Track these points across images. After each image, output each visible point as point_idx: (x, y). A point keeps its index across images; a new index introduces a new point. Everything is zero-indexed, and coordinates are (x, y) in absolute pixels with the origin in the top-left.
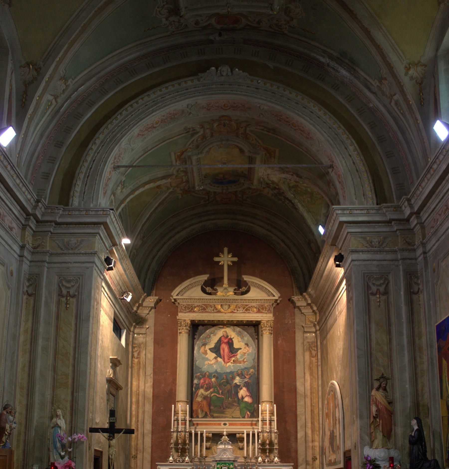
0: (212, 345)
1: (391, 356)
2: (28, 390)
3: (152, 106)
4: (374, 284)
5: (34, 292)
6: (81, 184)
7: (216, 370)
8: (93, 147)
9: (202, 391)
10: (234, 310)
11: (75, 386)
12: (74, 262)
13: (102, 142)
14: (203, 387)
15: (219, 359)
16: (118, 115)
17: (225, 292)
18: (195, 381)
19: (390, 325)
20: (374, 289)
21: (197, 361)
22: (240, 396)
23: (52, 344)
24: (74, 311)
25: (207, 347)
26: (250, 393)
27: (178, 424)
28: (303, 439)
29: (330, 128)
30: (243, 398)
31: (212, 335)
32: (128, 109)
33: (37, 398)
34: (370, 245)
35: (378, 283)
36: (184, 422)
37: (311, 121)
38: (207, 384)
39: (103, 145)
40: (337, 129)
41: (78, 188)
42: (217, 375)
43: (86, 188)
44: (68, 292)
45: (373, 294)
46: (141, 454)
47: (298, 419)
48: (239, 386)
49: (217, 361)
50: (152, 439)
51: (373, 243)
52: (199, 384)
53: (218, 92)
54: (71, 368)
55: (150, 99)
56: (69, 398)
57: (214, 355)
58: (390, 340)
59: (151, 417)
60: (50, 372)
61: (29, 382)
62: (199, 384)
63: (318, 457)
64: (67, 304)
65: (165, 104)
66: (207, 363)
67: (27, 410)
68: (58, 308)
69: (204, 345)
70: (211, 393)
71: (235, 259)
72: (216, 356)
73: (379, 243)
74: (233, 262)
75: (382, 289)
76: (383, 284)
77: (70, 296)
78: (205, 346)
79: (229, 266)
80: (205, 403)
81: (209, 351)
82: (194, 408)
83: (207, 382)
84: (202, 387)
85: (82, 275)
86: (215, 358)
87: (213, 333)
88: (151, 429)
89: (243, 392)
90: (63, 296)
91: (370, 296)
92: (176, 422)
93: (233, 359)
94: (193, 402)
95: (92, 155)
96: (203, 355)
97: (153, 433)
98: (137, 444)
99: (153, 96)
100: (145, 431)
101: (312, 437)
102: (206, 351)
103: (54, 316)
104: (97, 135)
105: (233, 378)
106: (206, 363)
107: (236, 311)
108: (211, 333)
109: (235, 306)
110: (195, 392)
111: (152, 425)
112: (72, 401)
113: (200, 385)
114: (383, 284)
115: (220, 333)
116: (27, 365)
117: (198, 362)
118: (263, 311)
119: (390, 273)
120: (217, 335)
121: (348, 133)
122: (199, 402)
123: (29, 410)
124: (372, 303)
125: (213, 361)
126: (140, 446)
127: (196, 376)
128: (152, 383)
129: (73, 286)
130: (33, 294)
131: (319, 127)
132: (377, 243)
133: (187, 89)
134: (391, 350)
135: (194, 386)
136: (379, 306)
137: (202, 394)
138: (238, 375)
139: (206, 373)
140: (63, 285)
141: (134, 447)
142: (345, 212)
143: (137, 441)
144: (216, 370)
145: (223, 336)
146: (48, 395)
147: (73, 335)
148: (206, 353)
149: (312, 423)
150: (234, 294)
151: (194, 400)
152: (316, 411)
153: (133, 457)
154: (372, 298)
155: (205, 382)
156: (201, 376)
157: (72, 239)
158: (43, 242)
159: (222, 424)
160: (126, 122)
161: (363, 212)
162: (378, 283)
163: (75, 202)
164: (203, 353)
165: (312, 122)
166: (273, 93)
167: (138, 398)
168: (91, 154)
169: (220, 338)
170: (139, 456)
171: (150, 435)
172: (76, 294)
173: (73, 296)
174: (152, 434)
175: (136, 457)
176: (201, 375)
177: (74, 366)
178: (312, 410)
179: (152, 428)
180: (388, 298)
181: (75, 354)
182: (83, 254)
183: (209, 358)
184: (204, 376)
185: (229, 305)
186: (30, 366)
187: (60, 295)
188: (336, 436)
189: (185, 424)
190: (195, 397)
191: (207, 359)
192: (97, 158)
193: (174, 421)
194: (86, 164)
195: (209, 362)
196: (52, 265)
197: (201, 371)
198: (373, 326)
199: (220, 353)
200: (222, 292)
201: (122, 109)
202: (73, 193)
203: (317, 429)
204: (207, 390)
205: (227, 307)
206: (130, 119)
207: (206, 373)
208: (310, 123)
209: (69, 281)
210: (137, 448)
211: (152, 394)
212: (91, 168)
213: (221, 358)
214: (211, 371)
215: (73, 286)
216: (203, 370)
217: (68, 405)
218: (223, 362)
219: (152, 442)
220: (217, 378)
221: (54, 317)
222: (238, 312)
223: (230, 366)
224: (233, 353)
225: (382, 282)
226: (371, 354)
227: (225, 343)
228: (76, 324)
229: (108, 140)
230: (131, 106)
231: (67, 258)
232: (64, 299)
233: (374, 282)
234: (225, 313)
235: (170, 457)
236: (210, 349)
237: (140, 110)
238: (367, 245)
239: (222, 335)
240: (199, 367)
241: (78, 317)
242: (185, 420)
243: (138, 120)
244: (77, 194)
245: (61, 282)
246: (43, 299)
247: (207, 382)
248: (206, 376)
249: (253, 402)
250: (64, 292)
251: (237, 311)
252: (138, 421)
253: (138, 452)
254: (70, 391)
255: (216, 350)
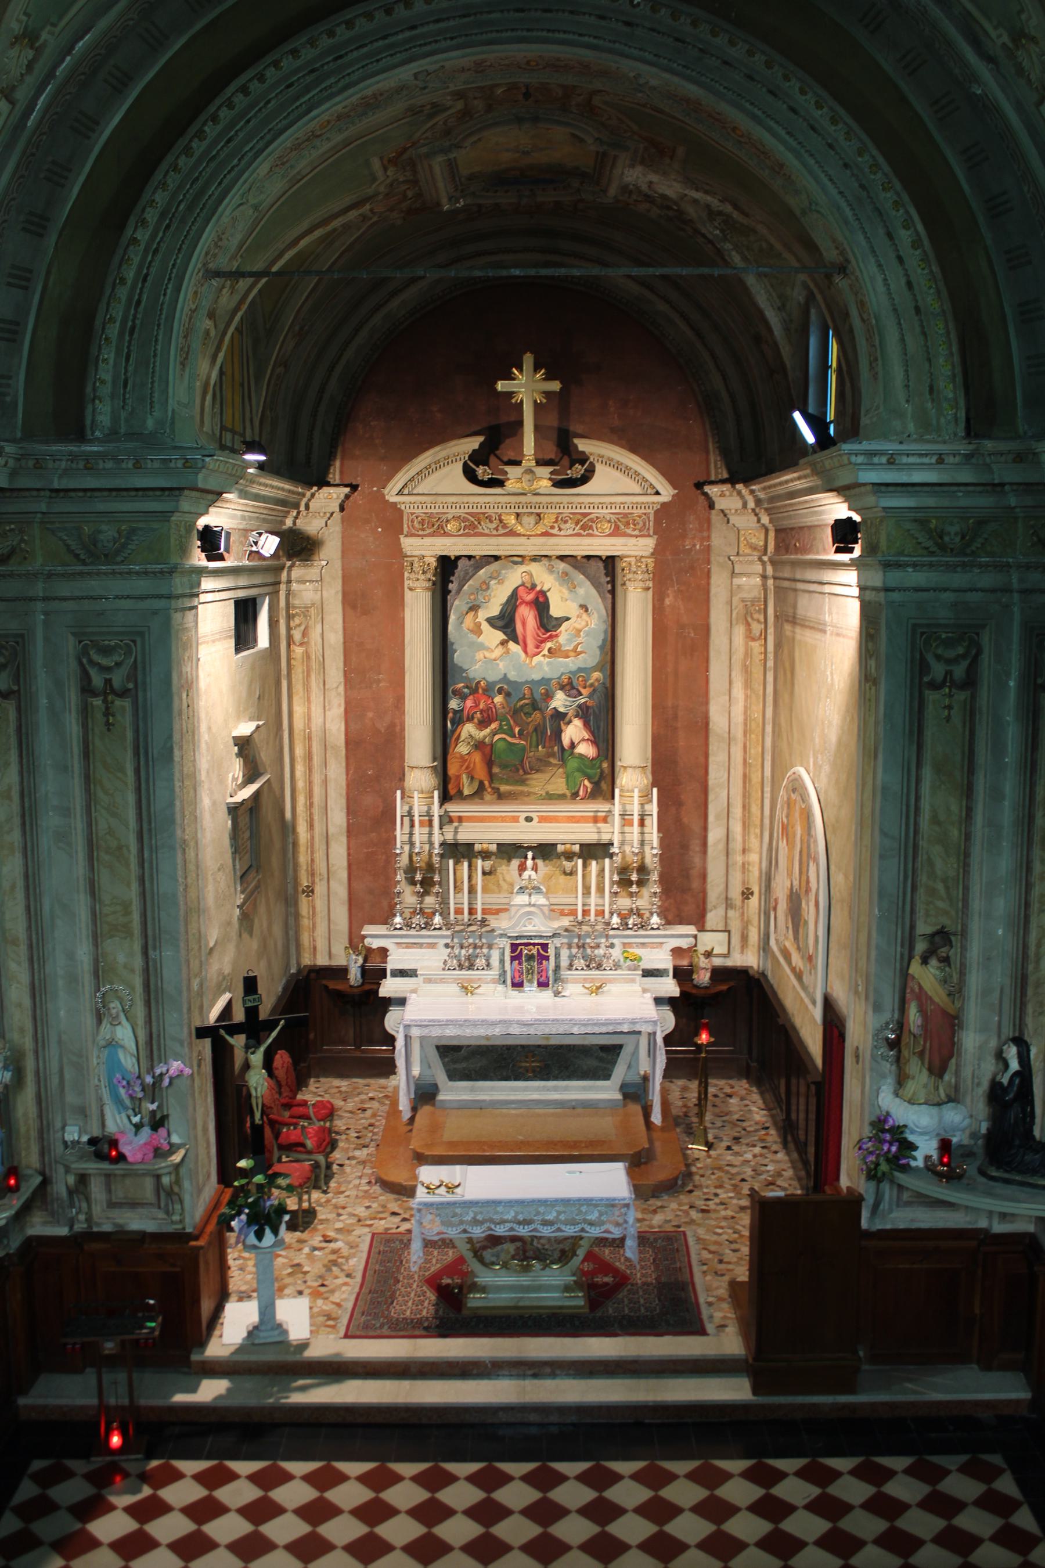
0: (494, 610)
1: (967, 855)
2: (30, 946)
3: (307, 89)
4: (938, 658)
5: (15, 688)
6: (112, 355)
7: (505, 674)
8: (138, 235)
9: (469, 729)
10: (552, 527)
11: (150, 933)
12: (117, 597)
13: (163, 215)
14: (473, 718)
15: (511, 645)
16: (205, 124)
17: (529, 479)
18: (453, 704)
19: (971, 770)
20: (938, 670)
21: (455, 651)
22: (566, 742)
23: (79, 824)
24: (129, 735)
25: (482, 615)
26: (592, 733)
27: (412, 826)
28: (722, 846)
29: (846, 166)
30: (573, 746)
31: (493, 582)
32: (236, 100)
33: (57, 966)
34: (936, 544)
35: (951, 654)
36: (427, 818)
37: (791, 140)
38: (482, 711)
39: (168, 227)
40: (867, 170)
41: (106, 370)
42: (507, 688)
43: (130, 369)
44: (108, 681)
45: (934, 686)
46: (325, 882)
47: (711, 797)
48: (565, 715)
49: (508, 652)
50: (349, 848)
51: (946, 539)
52: (462, 710)
53: (509, 34)
54: (135, 886)
55: (299, 63)
56: (138, 962)
57: (500, 636)
58: (969, 811)
59: (344, 792)
60: (82, 896)
61: (29, 928)
62: (462, 710)
63: (756, 889)
64: (107, 713)
65: (347, 80)
66: (482, 656)
67: (33, 996)
68: (85, 726)
69: (474, 608)
70: (494, 733)
71: (555, 386)
72: (505, 637)
73: (963, 537)
74: (547, 394)
75: (959, 671)
76: (964, 656)
77: (113, 691)
78: (477, 611)
79: (537, 407)
80: (477, 757)
81: (485, 626)
82: (452, 771)
83: (481, 706)
84: (470, 719)
85: (142, 634)
86: (503, 643)
87: (495, 578)
88: (345, 825)
89: (574, 731)
90: (94, 693)
91: (927, 692)
92: (406, 820)
93: (549, 645)
94: (449, 757)
95: (136, 260)
96: (472, 637)
97: (351, 831)
98: (312, 860)
99: (308, 54)
100: (331, 830)
101: (744, 841)
102: (480, 624)
103: (76, 749)
104: (146, 196)
105: (549, 696)
106: (480, 655)
107: (555, 531)
108: (492, 578)
109: (553, 518)
110: (453, 731)
111: (348, 813)
112: (146, 970)
113: (466, 712)
114: (964, 656)
115: (514, 577)
116: (20, 883)
117: (458, 657)
118: (629, 531)
119: (984, 626)
120: (506, 583)
121: (898, 186)
122: (462, 757)
123: (38, 999)
124: (930, 710)
126: (321, 866)
127: (455, 693)
129: (118, 664)
130: (13, 692)
131: (812, 162)
132: (958, 539)
133: (413, 27)
134: (968, 837)
135: (450, 715)
136: (948, 719)
137: (471, 736)
138: (562, 688)
139: (479, 682)
140: (91, 662)
141: (305, 868)
142: (876, 460)
143: (312, 853)
144: (505, 674)
145: (523, 585)
146: (84, 953)
147: (131, 798)
148: (478, 631)
149: (744, 807)
150: (550, 483)
151: (451, 751)
152: (756, 778)
153: (304, 892)
154: (931, 696)
155: (477, 706)
156: (466, 690)
157: (104, 527)
158: (22, 540)
159: (522, 819)
160: (231, 145)
161: (926, 460)
162: (951, 654)
163: (102, 414)
164: (472, 631)
165: (794, 144)
166: (677, 40)
167: (310, 747)
168: (135, 257)
169: (515, 591)
170: (320, 889)
171: (344, 839)
172: (131, 686)
173: (123, 694)
174: (348, 837)
175: (312, 891)
176: (467, 687)
177: (142, 881)
178: (745, 776)
179: (348, 820)
180: (973, 697)
181: (141, 851)
182: (137, 573)
183: (487, 644)
184: (474, 691)
185: (539, 515)
186: (27, 888)
187: (87, 690)
188: (806, 923)
189: (430, 823)
190: (453, 746)
191: (482, 647)
192: (153, 270)
193: (402, 817)
194: (122, 293)
195: (487, 654)
196: (56, 605)
197: (467, 678)
198: (927, 773)
199: (514, 630)
200: (519, 480)
201: (218, 102)
202: (94, 390)
203: (758, 822)
204: (483, 724)
205: (532, 520)
206: (241, 135)
207: (479, 682)
208: (791, 150)
209: (106, 651)
210: (313, 870)
211: (343, 737)
212: (139, 302)
213: (517, 642)
214: (493, 676)
215: (118, 664)
216: (471, 675)
217: (138, 982)
218: (523, 655)
219: (349, 855)
220: (508, 695)
221: (76, 750)
222: (562, 533)
223: (540, 664)
224: (548, 631)
225: (961, 650)
226: (916, 847)
227: (527, 603)
228: (137, 771)
229: (182, 207)
230: (244, 90)
231: (94, 586)
232: (98, 702)
233: (939, 651)
234: (529, 536)
235: (395, 915)
236: (490, 621)
237: (273, 102)
238: (929, 543)
239: (519, 583)
240: (461, 668)
241: (140, 749)
242: (429, 814)
243: (268, 137)
244: (105, 391)
245: (85, 652)
246: (44, 701)
247: (481, 706)
248: (480, 691)
249: (599, 755)
250: (97, 680)
251: (560, 529)
252: (311, 805)
253: (317, 880)
254: (137, 947)
255: (505, 622)
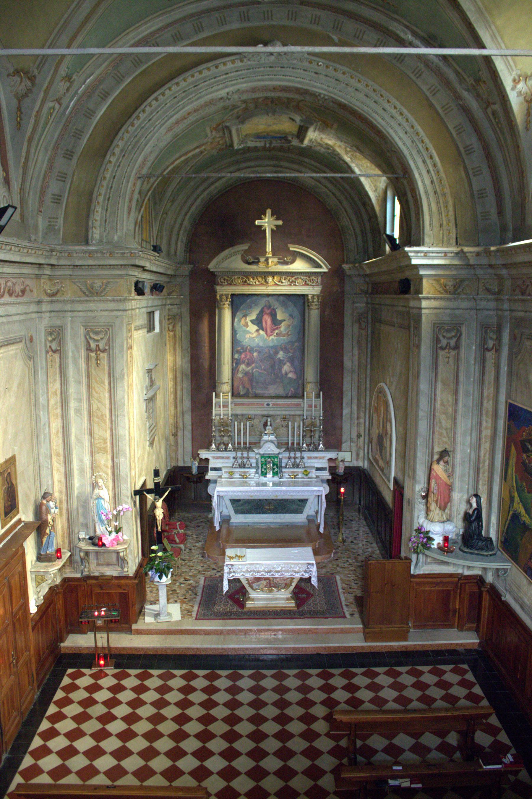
2: (65, 457)
9: (243, 367)
11: (115, 451)
15: (261, 332)
22: (284, 372)
23: (85, 405)
25: (248, 319)
28: (349, 416)
30: (286, 374)
33: (75, 465)
47: (344, 396)
48: (283, 360)
49: (259, 334)
54: (108, 432)
56: (110, 464)
57: (256, 327)
60: (86, 436)
67: (66, 478)
69: (245, 316)
70: (253, 369)
74: (277, 226)
79: (272, 231)
80: (246, 379)
81: (250, 324)
83: (248, 357)
86: (257, 331)
89: (287, 368)
93: (276, 331)
96: (244, 328)
105: (277, 353)
106: (248, 336)
112: (113, 467)
116: (61, 430)
122: (240, 378)
125: (255, 334)
128: (189, 358)
138: (282, 350)
145: (266, 306)
146: (87, 459)
148: (247, 325)
149: (358, 399)
155: (246, 357)
164: (244, 326)
177: (111, 430)
178: (358, 386)
186: (63, 432)
191: (249, 332)
199: (262, 325)
203: (363, 406)
204: (248, 365)
213: (263, 330)
214: (253, 345)
216: (244, 343)
217: (110, 472)
218: (265, 336)
220: (259, 352)
223: (273, 339)
224: (275, 325)
227: (268, 314)
236: (252, 322)
249: (297, 378)
254: (109, 457)
255: (258, 322)
